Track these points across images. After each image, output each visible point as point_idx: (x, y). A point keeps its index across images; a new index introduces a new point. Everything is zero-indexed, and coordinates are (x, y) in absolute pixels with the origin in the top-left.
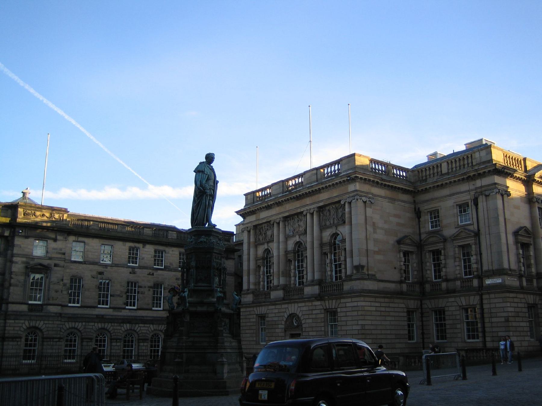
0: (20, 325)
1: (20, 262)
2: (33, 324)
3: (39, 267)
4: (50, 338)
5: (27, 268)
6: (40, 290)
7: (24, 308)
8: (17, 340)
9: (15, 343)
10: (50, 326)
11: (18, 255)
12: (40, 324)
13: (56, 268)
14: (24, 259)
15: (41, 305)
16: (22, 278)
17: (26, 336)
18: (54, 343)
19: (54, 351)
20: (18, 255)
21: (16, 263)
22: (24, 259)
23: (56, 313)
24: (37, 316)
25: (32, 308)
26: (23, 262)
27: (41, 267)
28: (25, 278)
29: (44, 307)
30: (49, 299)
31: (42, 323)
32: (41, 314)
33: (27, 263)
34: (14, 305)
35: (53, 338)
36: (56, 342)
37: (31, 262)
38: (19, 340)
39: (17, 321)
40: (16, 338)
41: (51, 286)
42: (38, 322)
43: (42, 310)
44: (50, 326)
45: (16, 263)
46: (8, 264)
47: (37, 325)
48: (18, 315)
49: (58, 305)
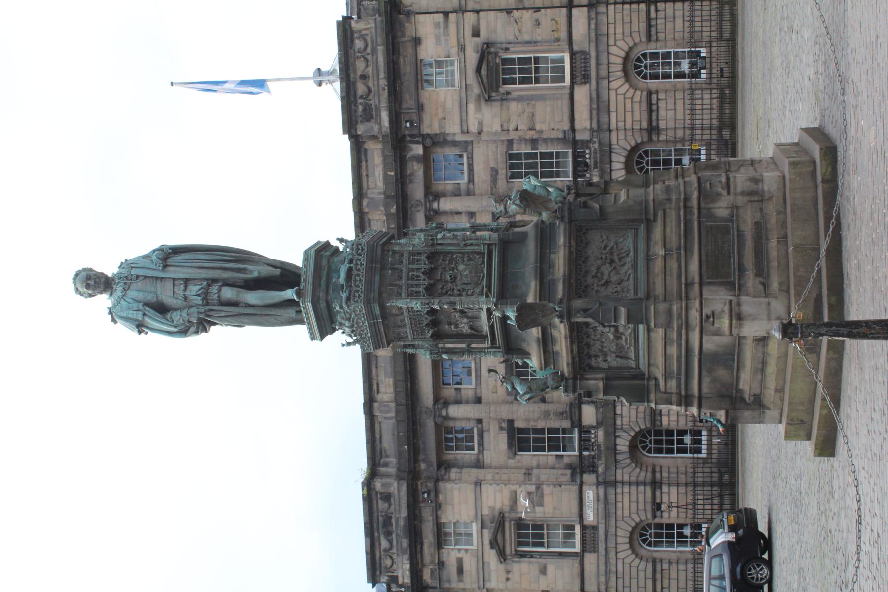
0: (620, 98)
1: (479, 116)
2: (617, 69)
3: (484, 72)
4: (649, 26)
5: (489, 99)
6: (537, 60)
7: (582, 94)
8: (654, 101)
9: (662, 104)
10: (619, 30)
11: (464, 121)
12: (617, 53)
13: (483, 33)
14: (471, 107)
15: (573, 55)
16: (514, 106)
17: (645, 78)
18: (661, 14)
19: (679, 13)
20: (464, 121)
21: (481, 124)
22: (471, 107)
23: (589, 19)
24: (598, 64)
25: (580, 75)
26: (478, 109)
27: (484, 67)
28: (514, 99)
29: (576, 48)
30: (558, 40)
31: (613, 50)
32: (593, 54)
33: (478, 99)
34: (577, 116)
35: (649, 19)
36: (657, 11)
37: (476, 90)
38: (654, 96)
39: (612, 108)
40: (650, 104)
41: (526, 37)
42: (613, 59)
43: (583, 53)
44: (619, 30)
45: (481, 124)
46: (484, 137)
47: (620, 61)
48: (599, 106)
49: (570, 16)
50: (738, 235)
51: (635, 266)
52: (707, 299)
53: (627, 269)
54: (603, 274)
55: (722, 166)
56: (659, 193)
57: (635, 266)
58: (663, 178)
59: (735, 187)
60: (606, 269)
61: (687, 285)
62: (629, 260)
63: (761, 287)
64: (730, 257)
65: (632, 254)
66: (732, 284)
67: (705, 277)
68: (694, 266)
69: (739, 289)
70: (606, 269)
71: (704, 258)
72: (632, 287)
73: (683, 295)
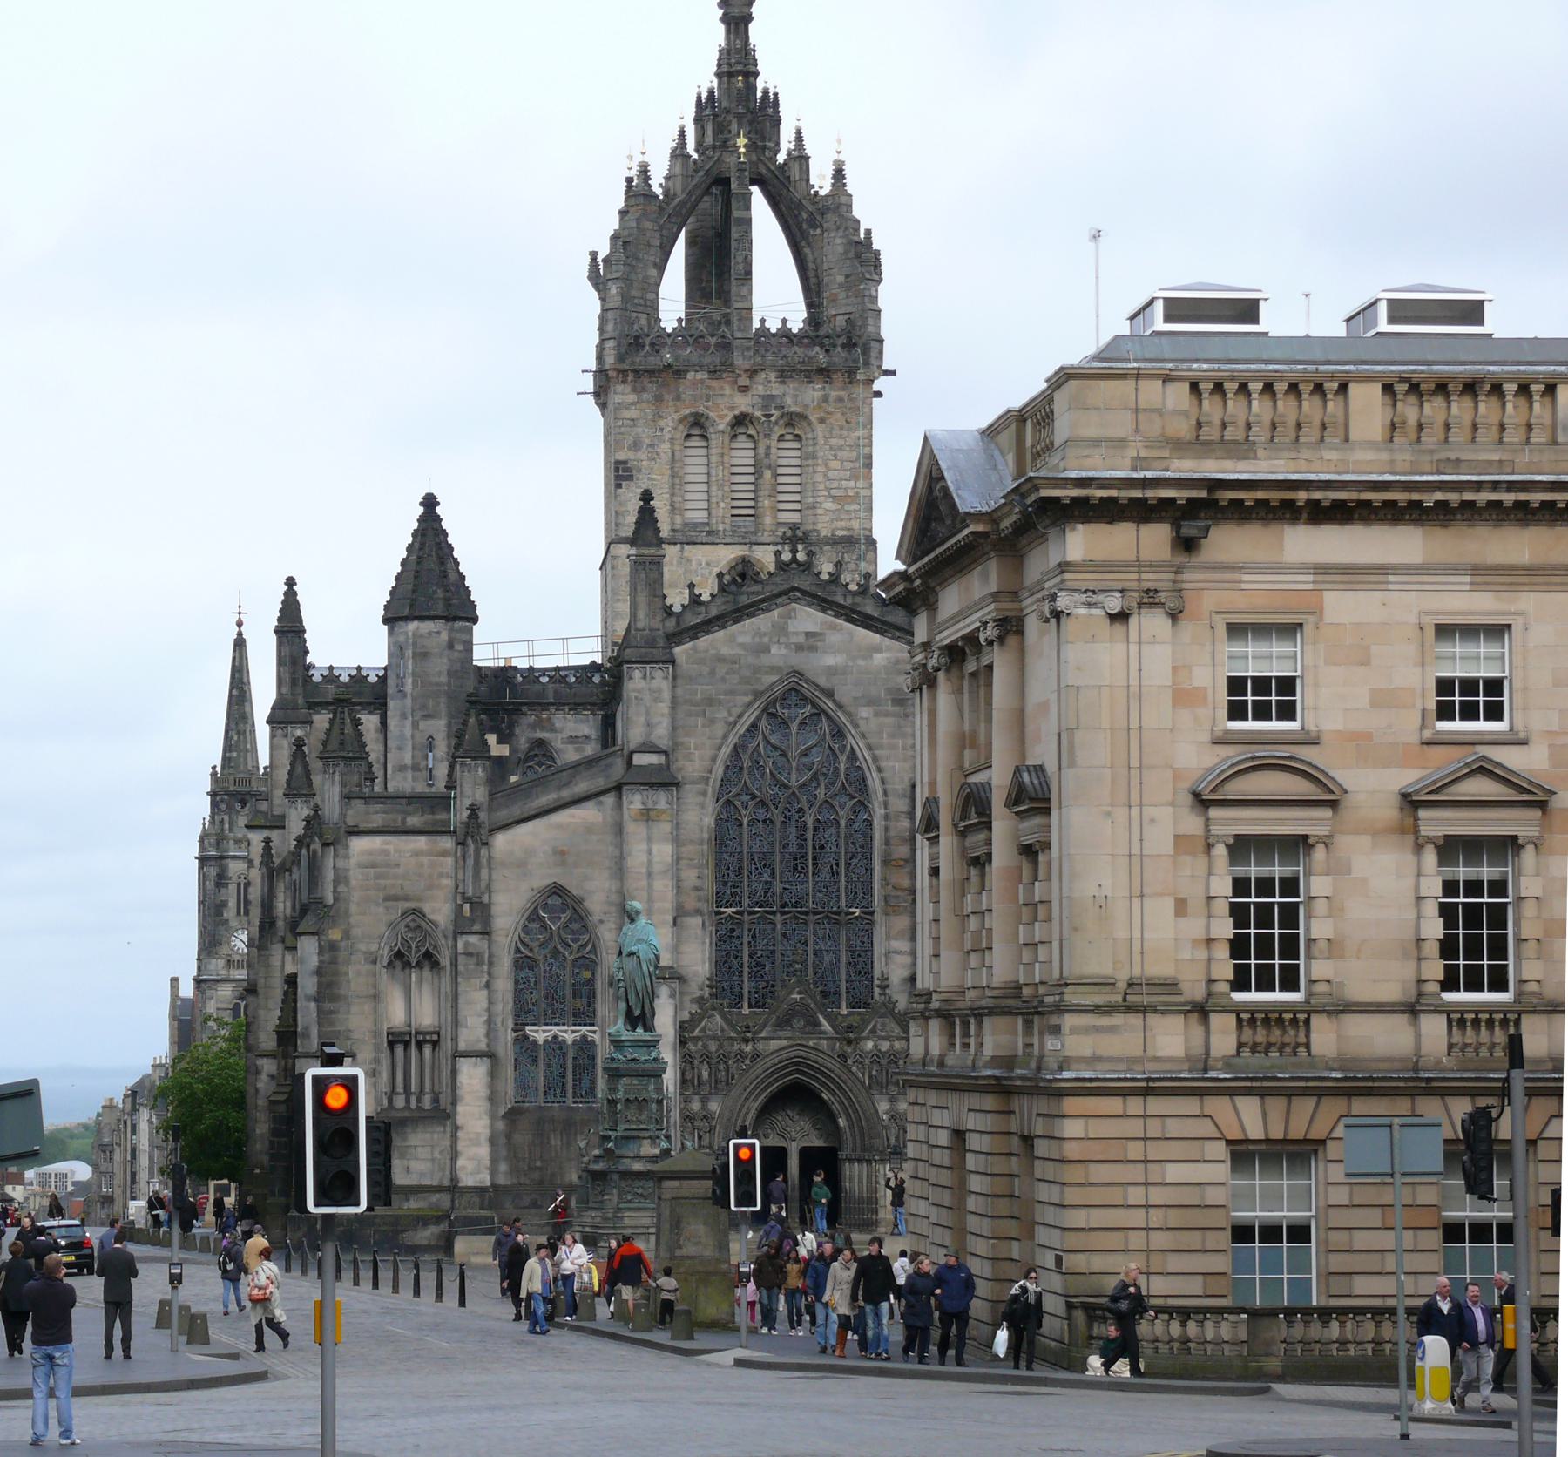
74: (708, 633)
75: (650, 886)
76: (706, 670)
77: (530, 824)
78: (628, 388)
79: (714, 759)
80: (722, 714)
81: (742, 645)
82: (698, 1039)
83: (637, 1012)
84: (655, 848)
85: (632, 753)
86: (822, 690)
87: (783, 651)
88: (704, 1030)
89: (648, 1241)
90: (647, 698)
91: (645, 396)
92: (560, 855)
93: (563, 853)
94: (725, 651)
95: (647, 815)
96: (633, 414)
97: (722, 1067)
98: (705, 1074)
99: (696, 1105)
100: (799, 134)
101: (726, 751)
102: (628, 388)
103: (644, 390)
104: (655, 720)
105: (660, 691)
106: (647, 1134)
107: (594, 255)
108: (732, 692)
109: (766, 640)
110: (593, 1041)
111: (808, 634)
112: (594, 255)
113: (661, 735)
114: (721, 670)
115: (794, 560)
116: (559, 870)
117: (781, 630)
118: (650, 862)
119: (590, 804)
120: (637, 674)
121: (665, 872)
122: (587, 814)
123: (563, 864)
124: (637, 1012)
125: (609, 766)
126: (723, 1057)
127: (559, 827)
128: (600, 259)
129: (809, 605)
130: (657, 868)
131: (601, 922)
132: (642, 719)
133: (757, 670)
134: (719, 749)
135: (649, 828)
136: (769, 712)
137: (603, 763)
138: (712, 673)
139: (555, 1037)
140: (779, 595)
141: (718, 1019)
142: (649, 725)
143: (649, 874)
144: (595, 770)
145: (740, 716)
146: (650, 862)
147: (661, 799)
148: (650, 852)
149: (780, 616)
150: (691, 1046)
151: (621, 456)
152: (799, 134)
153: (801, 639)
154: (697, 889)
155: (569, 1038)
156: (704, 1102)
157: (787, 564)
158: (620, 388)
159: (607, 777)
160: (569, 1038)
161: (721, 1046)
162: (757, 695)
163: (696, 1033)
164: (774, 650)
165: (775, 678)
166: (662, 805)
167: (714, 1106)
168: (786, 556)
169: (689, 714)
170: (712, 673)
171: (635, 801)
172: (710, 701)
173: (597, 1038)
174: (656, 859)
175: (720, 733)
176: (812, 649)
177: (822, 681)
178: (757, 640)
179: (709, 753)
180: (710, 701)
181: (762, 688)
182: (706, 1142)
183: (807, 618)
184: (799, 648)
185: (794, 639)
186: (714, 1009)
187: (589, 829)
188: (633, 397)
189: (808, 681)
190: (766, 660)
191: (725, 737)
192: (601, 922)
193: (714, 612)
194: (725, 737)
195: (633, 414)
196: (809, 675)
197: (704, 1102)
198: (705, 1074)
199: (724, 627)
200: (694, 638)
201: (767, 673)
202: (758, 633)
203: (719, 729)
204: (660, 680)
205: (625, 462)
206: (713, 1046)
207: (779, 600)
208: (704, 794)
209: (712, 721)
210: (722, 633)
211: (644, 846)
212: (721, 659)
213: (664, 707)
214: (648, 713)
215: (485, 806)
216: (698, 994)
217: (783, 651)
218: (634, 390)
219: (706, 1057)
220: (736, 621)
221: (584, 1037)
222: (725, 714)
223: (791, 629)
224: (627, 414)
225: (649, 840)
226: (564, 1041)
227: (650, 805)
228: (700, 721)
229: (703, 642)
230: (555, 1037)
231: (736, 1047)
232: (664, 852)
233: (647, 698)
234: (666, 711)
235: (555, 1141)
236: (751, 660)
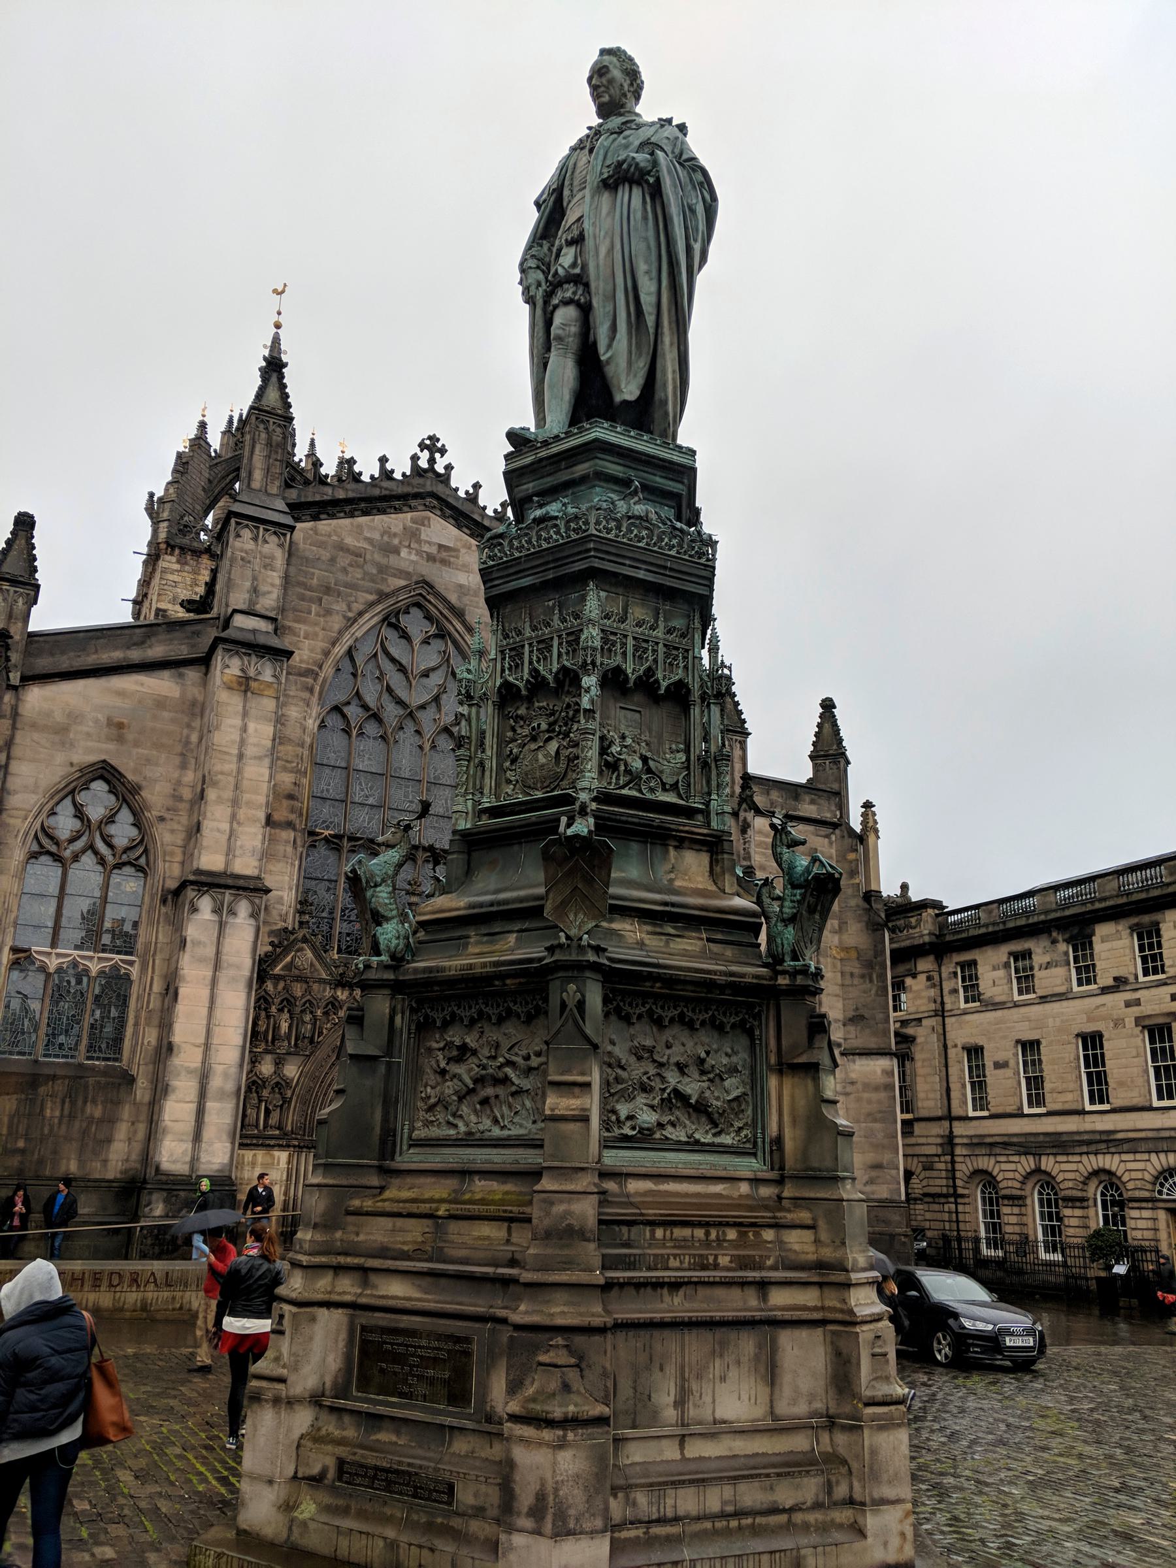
50: (442, 1426)
51: (470, 1140)
52: (313, 1319)
53: (471, 1120)
54: (459, 1060)
55: (847, 1409)
56: (559, 1209)
57: (470, 1140)
58: (821, 1223)
59: (525, 1441)
60: (465, 1072)
61: (364, 1271)
62: (487, 1123)
63: (315, 1470)
64: (401, 1395)
65: (496, 1132)
66: (341, 1390)
67: (365, 1318)
68: (396, 1290)
69: (332, 1409)
70: (465, 1072)
71: (406, 1321)
72: (435, 1132)
73: (342, 1260)
74: (332, 516)
75: (239, 771)
76: (325, 555)
77: (80, 684)
78: (174, 559)
79: (327, 653)
80: (340, 606)
81: (370, 541)
82: (278, 978)
83: (628, 390)
84: (252, 726)
85: (235, 611)
86: (452, 608)
87: (413, 557)
88: (289, 967)
89: (770, 1371)
90: (257, 563)
91: (187, 568)
92: (117, 728)
93: (120, 726)
94: (349, 541)
95: (245, 685)
96: (175, 577)
97: (307, 1018)
98: (284, 1027)
99: (266, 1068)
100: (312, 444)
101: (340, 650)
102: (174, 559)
103: (186, 563)
104: (263, 588)
105: (273, 558)
106: (695, 826)
107: (151, 495)
108: (354, 587)
109: (396, 541)
110: (127, 977)
111: (440, 546)
112: (151, 495)
113: (269, 602)
114: (344, 560)
115: (431, 469)
116: (111, 746)
117: (413, 535)
118: (242, 742)
119: (166, 674)
120: (247, 534)
121: (260, 758)
122: (161, 685)
123: (120, 739)
124: (628, 390)
125: (197, 634)
126: (310, 1005)
127: (121, 693)
128: (155, 499)
129: (444, 516)
130: (250, 751)
131: (162, 819)
132: (248, 584)
133: (383, 569)
134: (334, 644)
135: (245, 700)
136: (391, 620)
137: (189, 629)
138: (333, 560)
139: (75, 964)
140: (416, 496)
141: (309, 954)
142: (255, 590)
143: (241, 756)
144: (177, 634)
145: (361, 614)
146: (242, 742)
147: (266, 671)
148: (244, 729)
149: (413, 521)
150: (269, 986)
151: (162, 606)
152: (312, 444)
153: (433, 550)
154: (291, 797)
155: (94, 968)
156: (279, 1063)
157: (425, 471)
158: (168, 558)
159: (193, 646)
160: (94, 968)
161: (308, 990)
162: (383, 596)
163: (277, 970)
164: (404, 553)
165: (403, 583)
166: (267, 675)
167: (291, 1070)
168: (423, 464)
169: (302, 598)
170: (333, 560)
171: (228, 667)
172: (327, 590)
173: (135, 972)
174: (252, 740)
175: (337, 627)
176: (444, 562)
177: (453, 598)
178: (386, 538)
179: (321, 645)
180: (327, 590)
181: (387, 590)
182: (274, 1119)
183: (441, 531)
184: (431, 558)
185: (426, 548)
186: (305, 940)
187: (161, 703)
188: (177, 567)
189: (438, 595)
190: (393, 560)
191: (341, 633)
192: (162, 819)
193: (341, 495)
194: (341, 633)
195: (175, 577)
196: (441, 588)
197: (279, 1063)
198: (284, 1027)
199: (351, 515)
200: (316, 518)
201: (394, 576)
202: (386, 532)
203: (336, 623)
204: (272, 547)
205: (165, 611)
206: (298, 990)
207: (413, 503)
208: (311, 690)
209: (328, 612)
210: (347, 521)
211: (238, 722)
212: (342, 548)
213: (275, 577)
214: (255, 578)
215: (21, 646)
216: (280, 925)
217: (413, 557)
218: (178, 562)
219: (288, 1003)
220: (366, 513)
221: (115, 967)
222: (345, 607)
223: (423, 537)
224: (171, 577)
225: (245, 714)
226: (86, 971)
227: (252, 672)
228: (314, 608)
229: (325, 525)
230: (75, 964)
231: (328, 993)
232: (261, 732)
233: (257, 563)
234: (278, 582)
235: (52, 1111)
236: (378, 557)
